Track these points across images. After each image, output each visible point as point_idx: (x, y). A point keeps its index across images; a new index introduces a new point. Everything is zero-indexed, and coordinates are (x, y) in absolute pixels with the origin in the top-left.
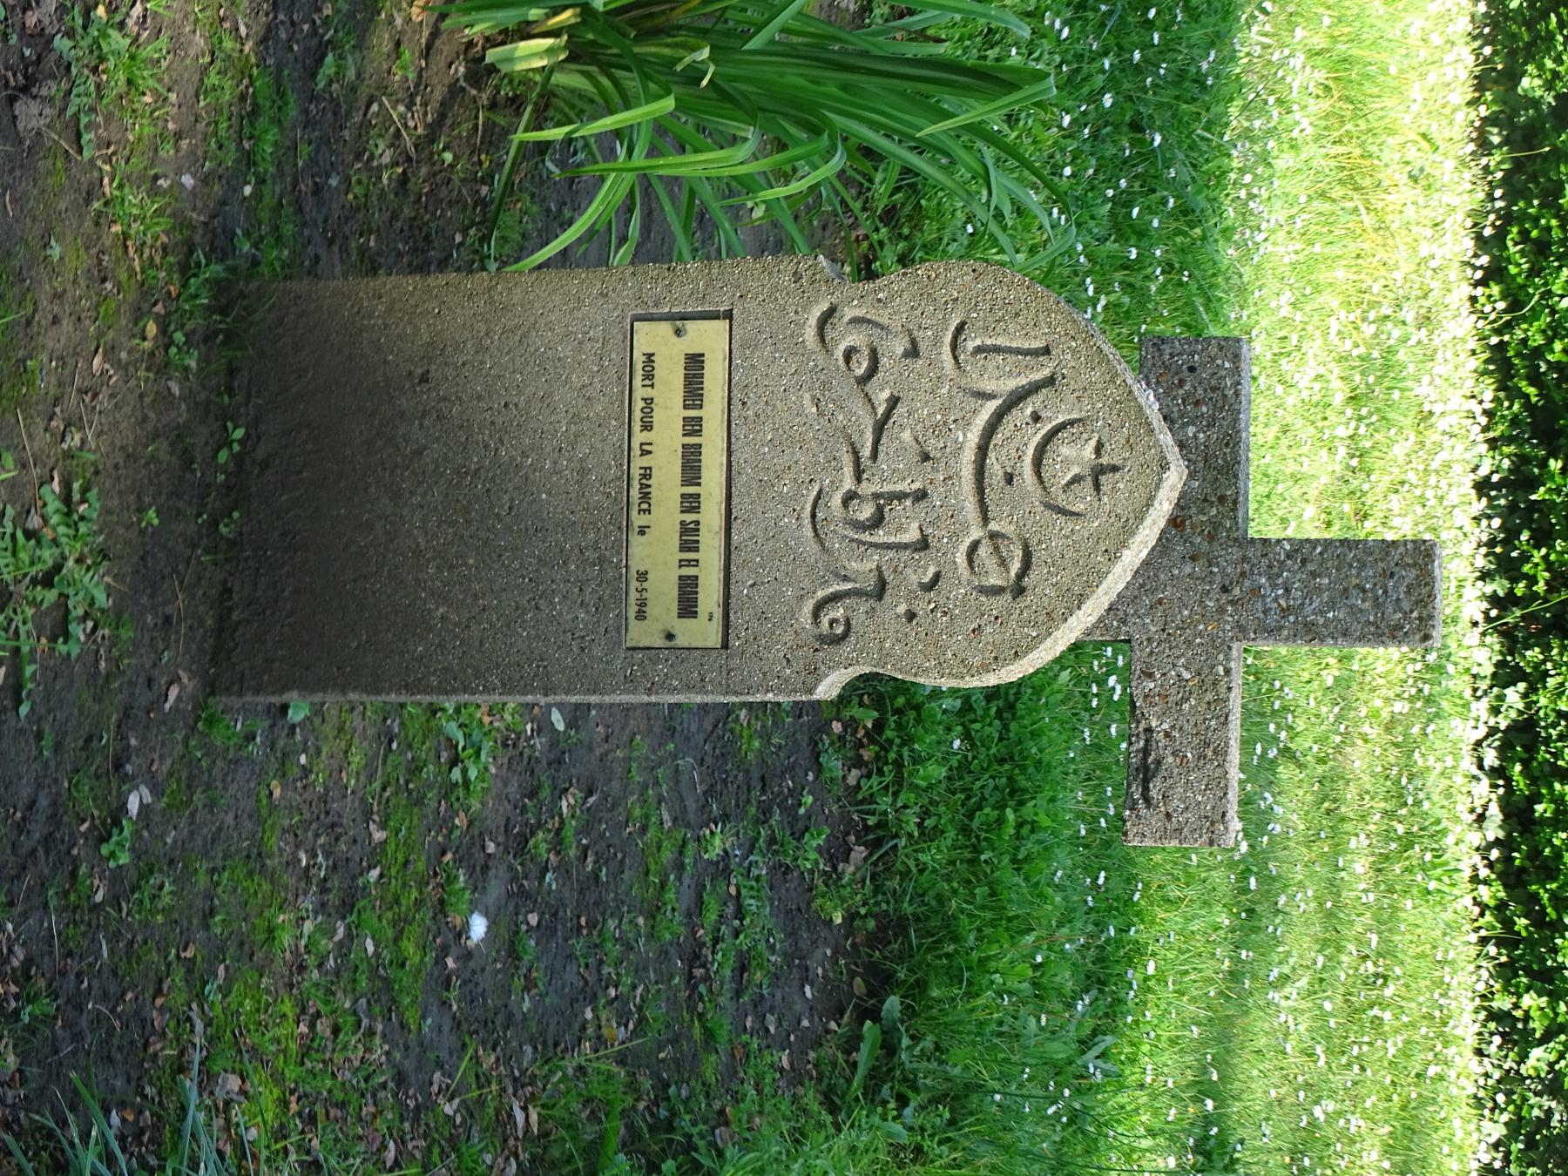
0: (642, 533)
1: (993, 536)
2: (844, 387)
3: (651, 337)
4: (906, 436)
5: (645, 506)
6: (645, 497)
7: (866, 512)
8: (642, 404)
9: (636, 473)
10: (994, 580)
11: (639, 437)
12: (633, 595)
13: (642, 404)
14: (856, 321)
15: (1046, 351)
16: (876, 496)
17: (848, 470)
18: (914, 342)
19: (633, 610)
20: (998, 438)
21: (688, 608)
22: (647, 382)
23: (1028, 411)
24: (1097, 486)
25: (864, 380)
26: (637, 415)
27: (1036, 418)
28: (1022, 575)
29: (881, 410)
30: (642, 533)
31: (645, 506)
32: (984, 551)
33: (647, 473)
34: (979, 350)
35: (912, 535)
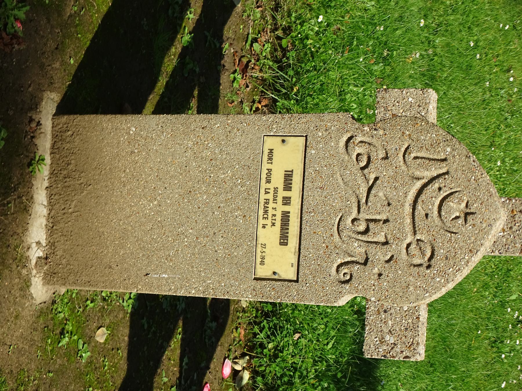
0: (264, 227)
2: (355, 169)
4: (381, 194)
6: (266, 212)
7: (362, 227)
8: (267, 171)
10: (417, 261)
12: (259, 254)
13: (267, 171)
14: (361, 142)
15: (445, 160)
19: (259, 260)
20: (423, 197)
22: (269, 161)
23: (437, 185)
24: (466, 220)
25: (363, 169)
26: (264, 176)
27: (440, 189)
28: (430, 259)
29: (371, 182)
31: (265, 216)
33: (267, 202)
34: (416, 158)
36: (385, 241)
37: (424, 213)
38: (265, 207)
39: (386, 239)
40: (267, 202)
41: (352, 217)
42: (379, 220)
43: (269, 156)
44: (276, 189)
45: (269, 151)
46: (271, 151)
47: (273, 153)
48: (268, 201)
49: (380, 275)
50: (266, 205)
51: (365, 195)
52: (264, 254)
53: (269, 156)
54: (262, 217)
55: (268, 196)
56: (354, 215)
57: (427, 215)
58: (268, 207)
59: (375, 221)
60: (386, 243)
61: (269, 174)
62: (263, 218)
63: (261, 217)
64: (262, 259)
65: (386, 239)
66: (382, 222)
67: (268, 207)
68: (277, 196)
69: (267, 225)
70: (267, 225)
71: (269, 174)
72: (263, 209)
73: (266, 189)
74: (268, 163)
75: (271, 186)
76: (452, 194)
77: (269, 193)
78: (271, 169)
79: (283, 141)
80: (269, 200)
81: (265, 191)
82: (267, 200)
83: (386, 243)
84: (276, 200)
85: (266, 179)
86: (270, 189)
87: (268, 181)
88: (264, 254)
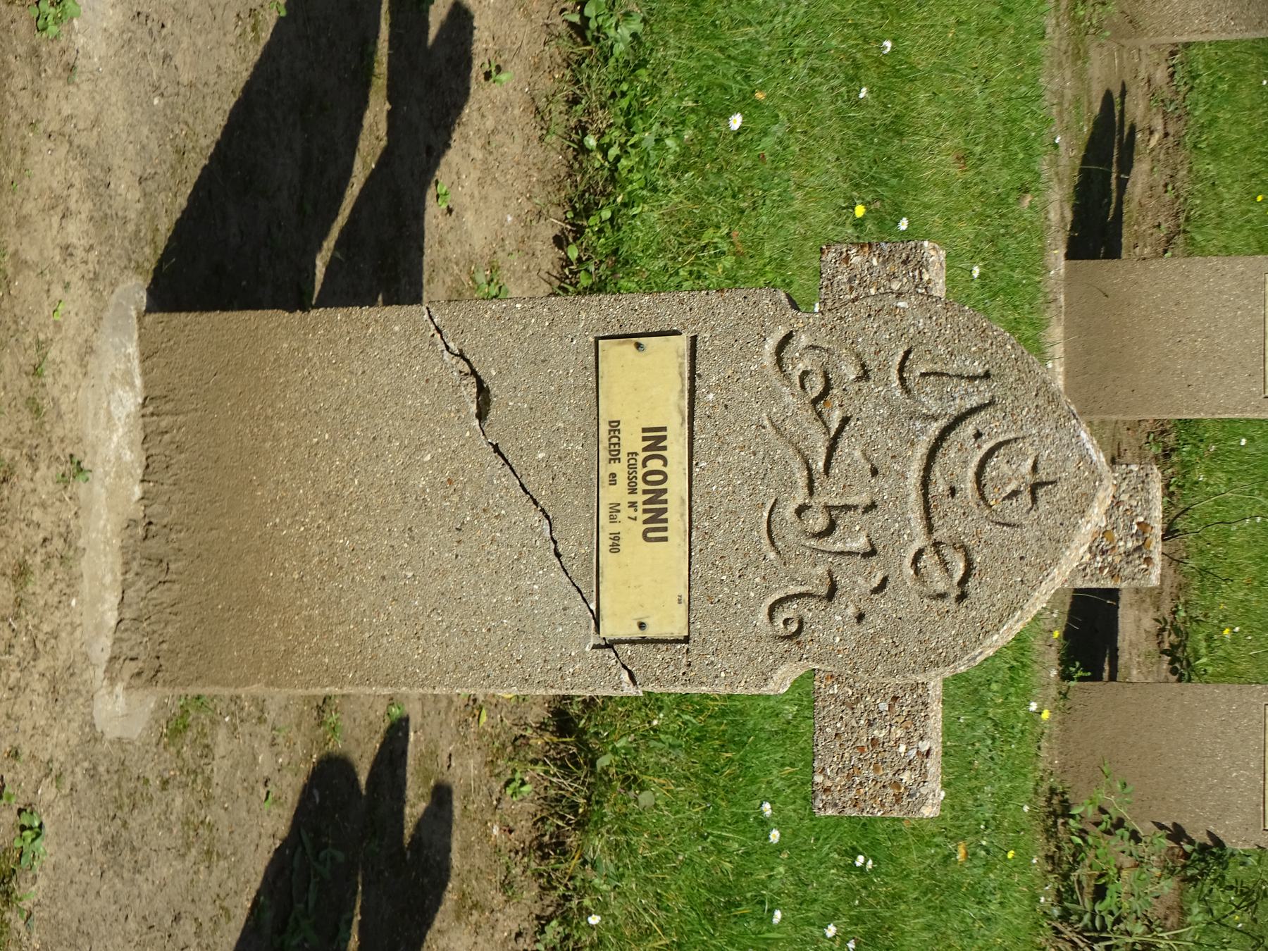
1: (936, 544)
7: (818, 521)
16: (828, 508)
17: (802, 481)
18: (863, 366)
25: (815, 402)
32: (929, 560)
35: (861, 543)
36: (869, 549)
37: (947, 487)
39: (872, 545)
41: (800, 501)
42: (856, 507)
49: (860, 617)
51: (822, 451)
56: (801, 496)
57: (953, 491)
59: (847, 508)
60: (873, 552)
65: (872, 545)
66: (860, 511)
76: (1007, 442)
79: (638, 346)
83: (873, 552)
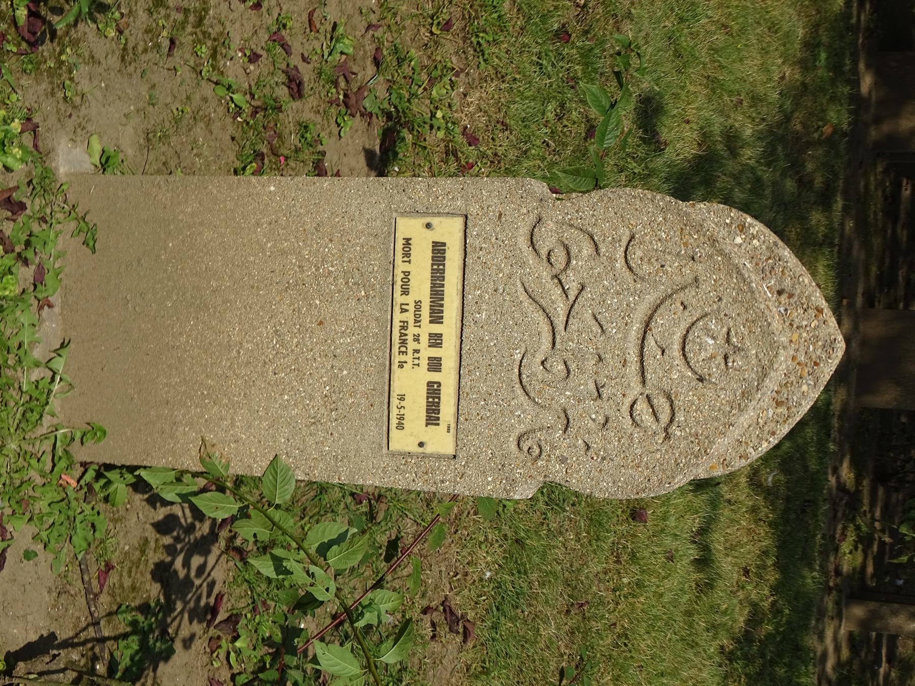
0: (401, 366)
3: (408, 227)
5: (403, 349)
6: (403, 343)
8: (402, 276)
9: (397, 325)
11: (399, 299)
12: (394, 412)
13: (402, 276)
21: (432, 416)
22: (406, 259)
26: (399, 283)
29: (573, 289)
30: (401, 367)
31: (403, 349)
33: (404, 326)
38: (402, 335)
40: (404, 326)
43: (405, 249)
44: (418, 304)
45: (404, 242)
46: (408, 241)
47: (410, 244)
48: (406, 324)
50: (403, 331)
52: (402, 411)
53: (405, 249)
54: (398, 350)
55: (404, 317)
58: (406, 335)
61: (406, 280)
62: (400, 352)
63: (395, 349)
64: (400, 419)
67: (406, 335)
68: (420, 315)
69: (406, 362)
70: (406, 362)
71: (406, 280)
72: (398, 338)
73: (402, 304)
74: (403, 261)
75: (410, 299)
77: (407, 311)
78: (409, 272)
80: (407, 322)
81: (402, 309)
82: (404, 322)
84: (420, 321)
85: (402, 285)
86: (408, 304)
87: (405, 292)
88: (402, 411)
